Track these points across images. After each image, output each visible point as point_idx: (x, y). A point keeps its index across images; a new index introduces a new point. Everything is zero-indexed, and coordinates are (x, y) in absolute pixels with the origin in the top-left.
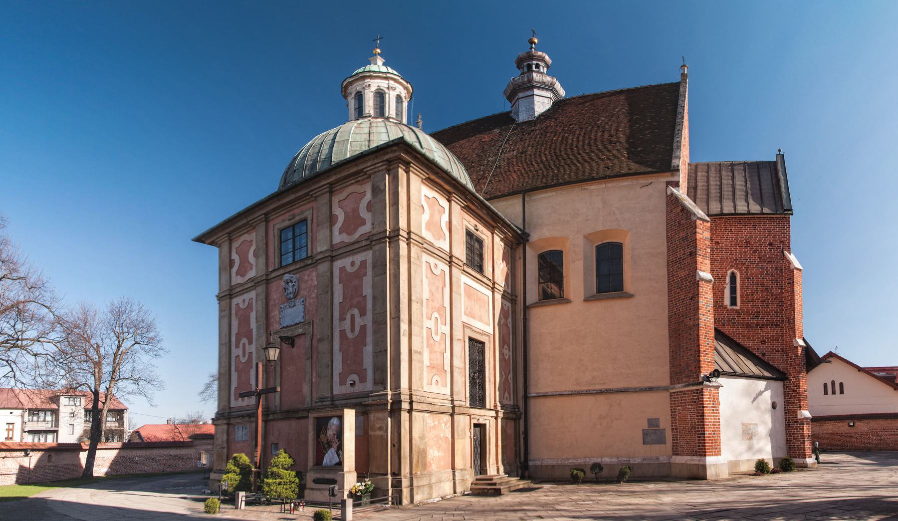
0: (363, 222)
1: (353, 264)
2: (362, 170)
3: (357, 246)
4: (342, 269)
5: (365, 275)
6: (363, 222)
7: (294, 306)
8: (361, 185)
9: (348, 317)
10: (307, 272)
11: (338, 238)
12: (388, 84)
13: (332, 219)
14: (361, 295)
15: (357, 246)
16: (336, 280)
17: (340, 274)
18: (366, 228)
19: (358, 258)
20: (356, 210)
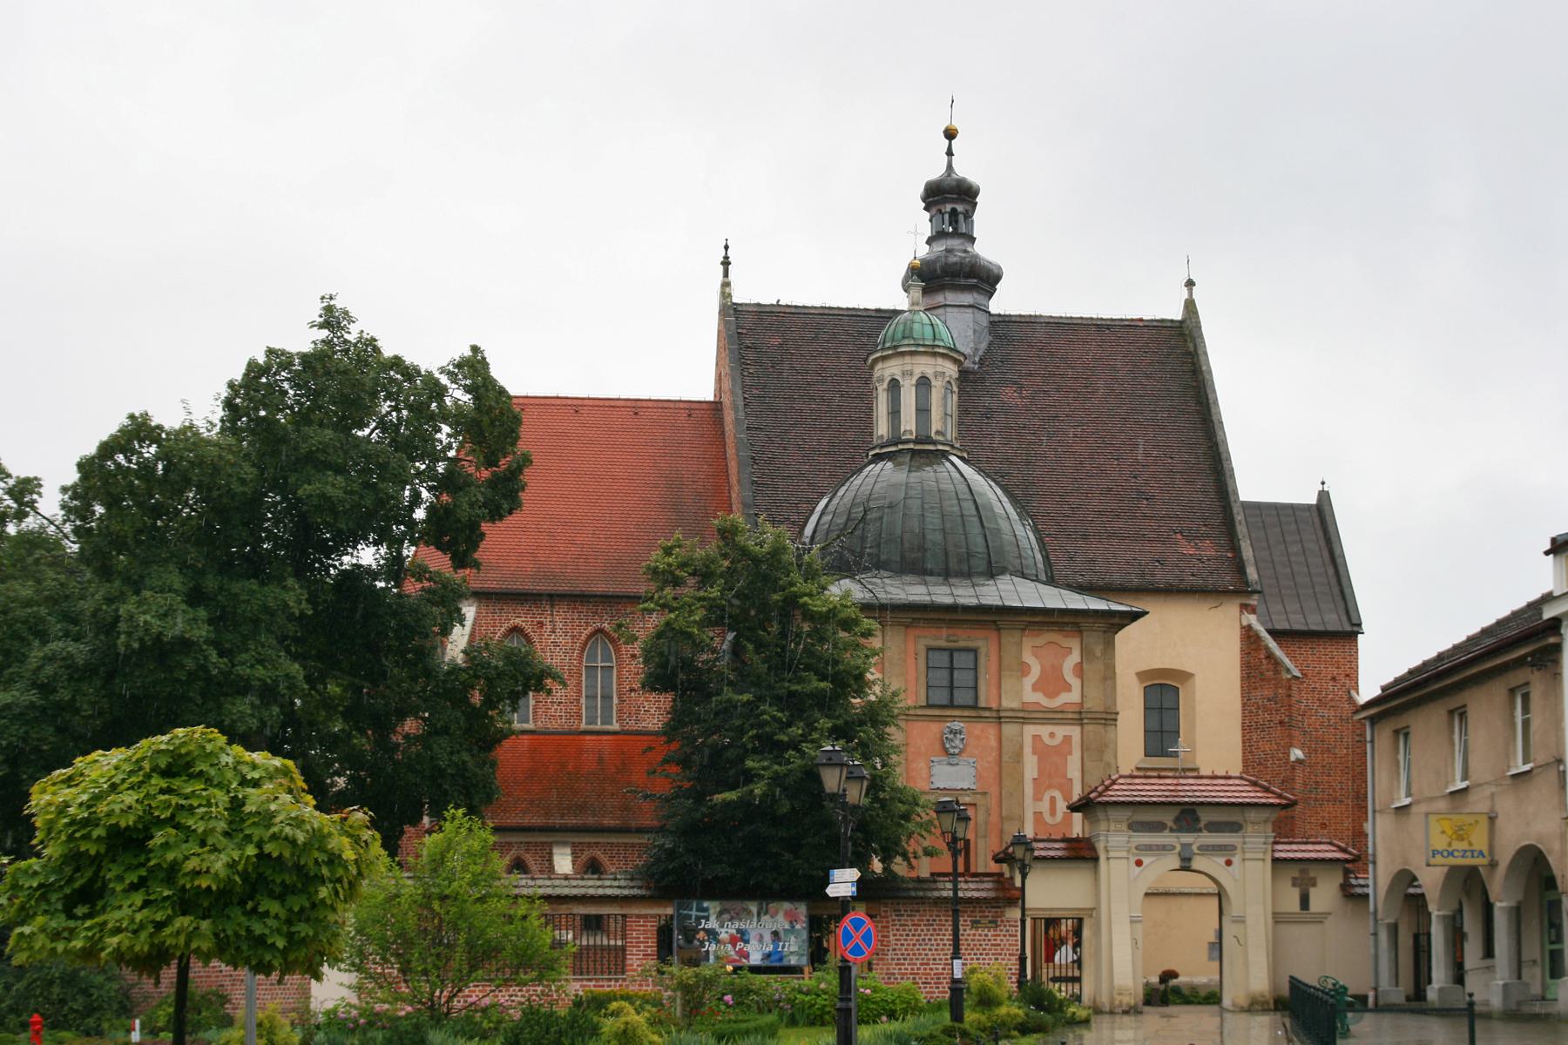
0: (1068, 688)
1: (1052, 735)
2: (1077, 623)
3: (1060, 716)
4: (1037, 738)
5: (1070, 753)
6: (1068, 688)
7: (957, 764)
8: (1066, 636)
9: (1047, 797)
10: (979, 726)
11: (1031, 696)
13: (1024, 669)
14: (1065, 776)
15: (1060, 716)
16: (1028, 749)
17: (1034, 744)
18: (1073, 696)
19: (1061, 731)
20: (1057, 669)
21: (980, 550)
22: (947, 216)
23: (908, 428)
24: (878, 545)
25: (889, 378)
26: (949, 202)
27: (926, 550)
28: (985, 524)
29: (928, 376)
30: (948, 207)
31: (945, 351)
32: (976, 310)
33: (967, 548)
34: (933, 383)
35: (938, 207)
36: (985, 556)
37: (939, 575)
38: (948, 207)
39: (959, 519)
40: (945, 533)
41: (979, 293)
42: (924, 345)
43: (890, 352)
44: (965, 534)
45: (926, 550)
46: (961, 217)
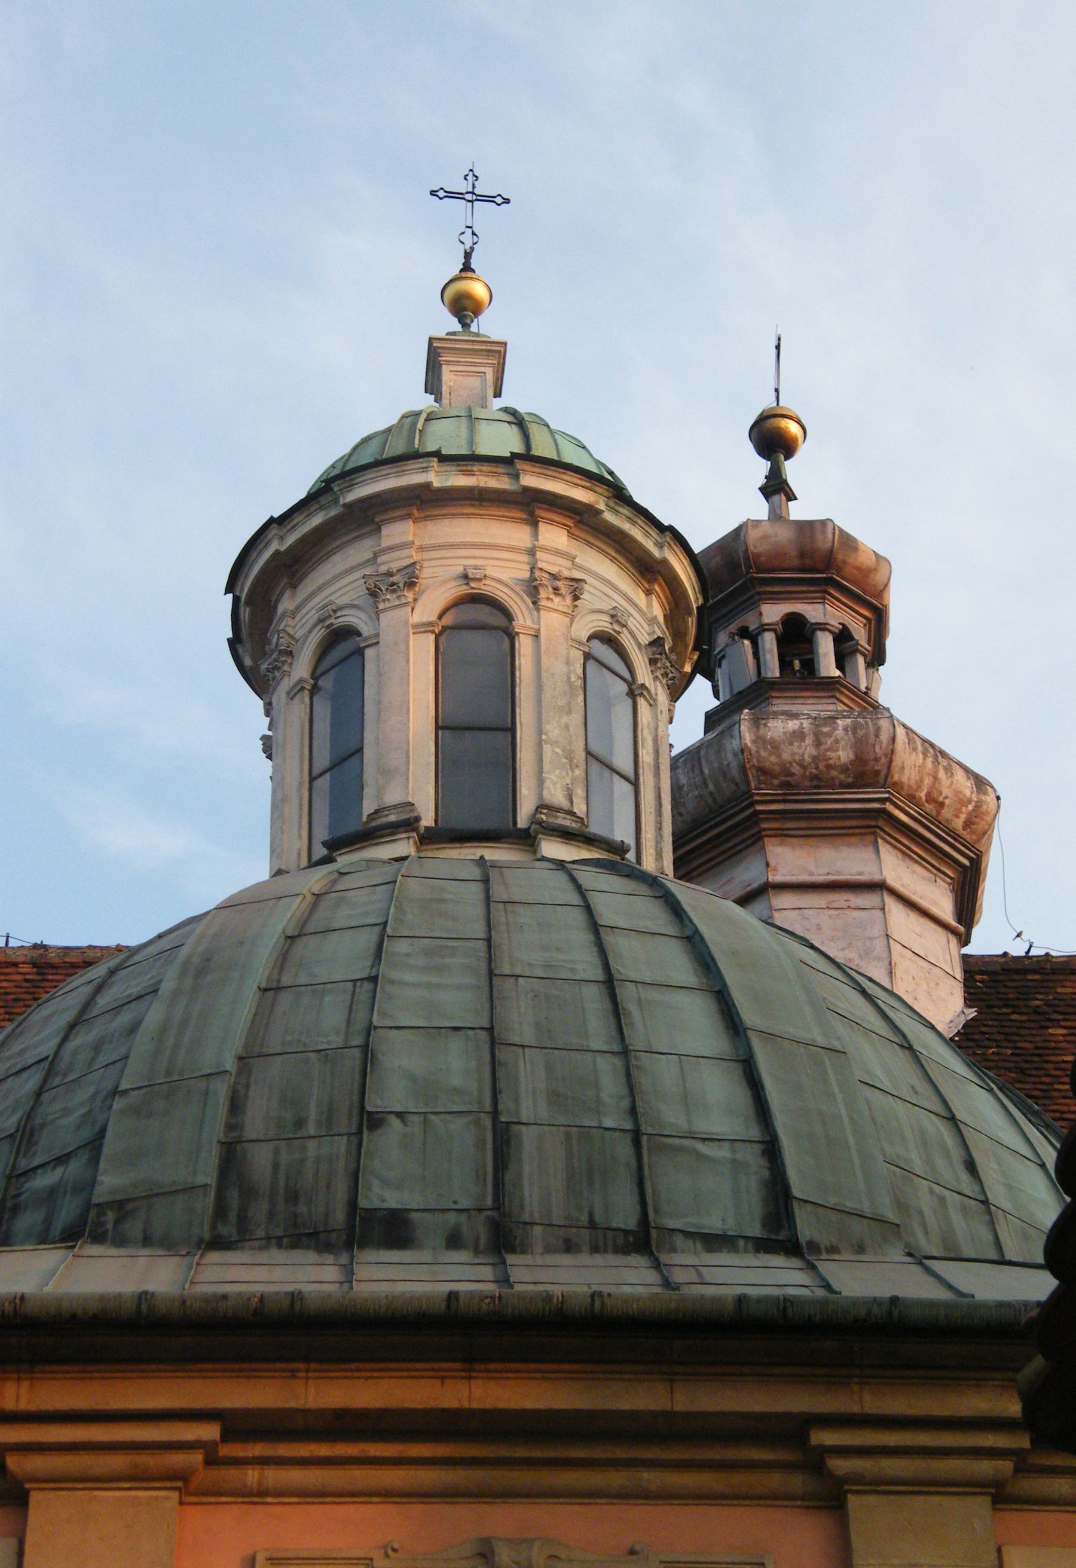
12: (532, 552)
21: (702, 1126)
22: (769, 641)
23: (393, 796)
24: (95, 1145)
25: (317, 636)
26: (776, 598)
27: (373, 1121)
28: (749, 1015)
29: (489, 588)
30: (773, 612)
31: (581, 495)
32: (891, 903)
33: (633, 1111)
34: (523, 619)
35: (733, 627)
36: (752, 1156)
37: (454, 1241)
38: (773, 612)
39: (593, 998)
40: (493, 1043)
41: (906, 854)
42: (470, 460)
43: (317, 520)
44: (625, 1053)
45: (373, 1121)
46: (825, 645)
